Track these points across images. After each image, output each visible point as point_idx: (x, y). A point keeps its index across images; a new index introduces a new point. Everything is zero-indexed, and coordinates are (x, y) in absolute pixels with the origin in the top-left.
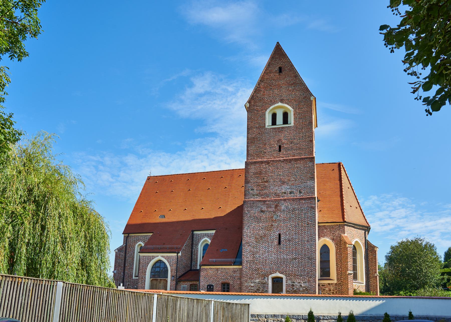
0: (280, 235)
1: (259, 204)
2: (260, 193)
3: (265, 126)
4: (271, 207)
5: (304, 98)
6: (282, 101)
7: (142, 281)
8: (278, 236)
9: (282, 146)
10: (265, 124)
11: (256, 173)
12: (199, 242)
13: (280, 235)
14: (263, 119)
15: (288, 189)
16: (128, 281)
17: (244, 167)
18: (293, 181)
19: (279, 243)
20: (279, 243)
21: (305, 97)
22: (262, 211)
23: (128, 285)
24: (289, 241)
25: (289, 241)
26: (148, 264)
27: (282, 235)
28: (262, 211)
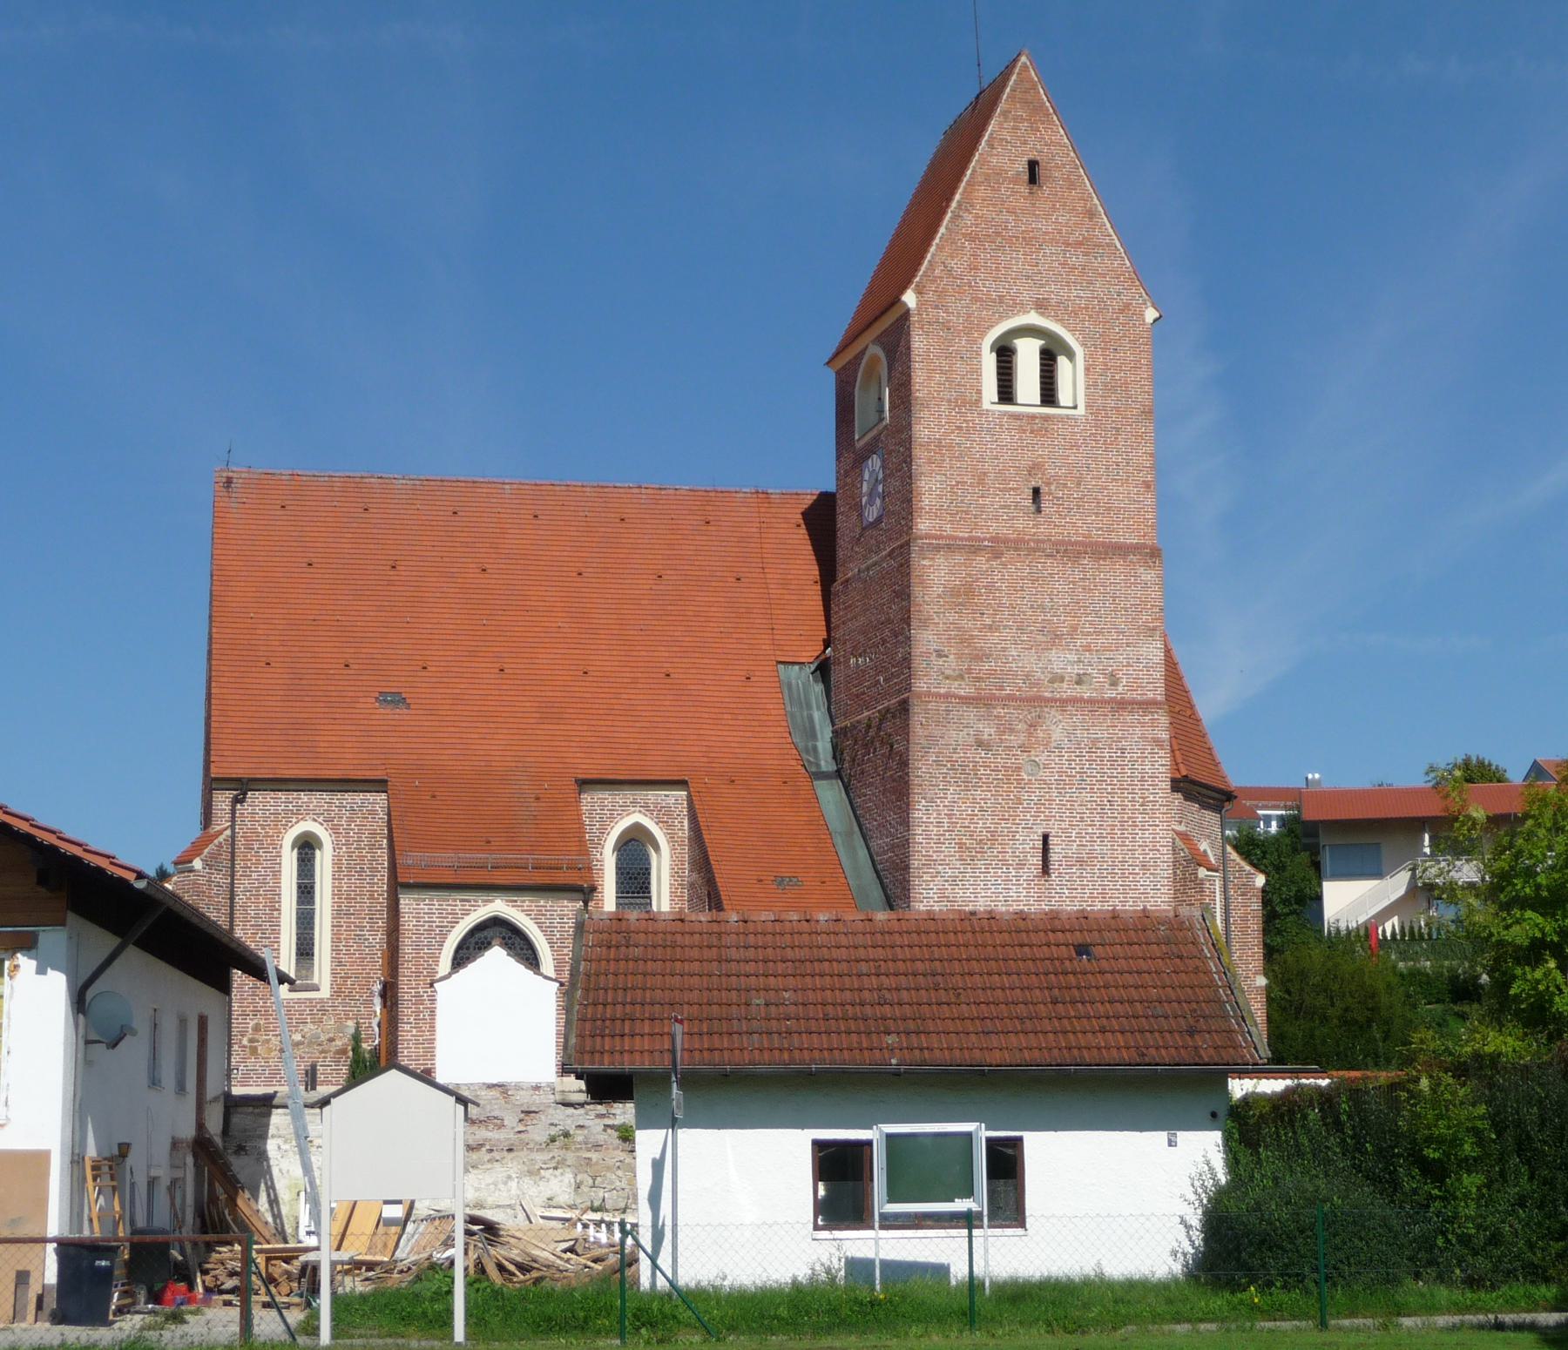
0: (1046, 838)
1: (970, 714)
2: (969, 671)
3: (979, 401)
4: (1012, 731)
5: (1121, 311)
6: (1041, 306)
7: (418, 1012)
8: (1039, 844)
9: (1044, 489)
10: (979, 392)
11: (954, 592)
12: (603, 831)
13: (1046, 838)
14: (972, 373)
15: (1072, 663)
16: (255, 1013)
17: (1326, 885)
18: (1089, 634)
19: (1046, 869)
20: (1046, 869)
21: (1127, 306)
22: (980, 744)
23: (257, 1028)
24: (1081, 861)
25: (1081, 861)
26: (444, 936)
27: (1052, 841)
28: (980, 744)
